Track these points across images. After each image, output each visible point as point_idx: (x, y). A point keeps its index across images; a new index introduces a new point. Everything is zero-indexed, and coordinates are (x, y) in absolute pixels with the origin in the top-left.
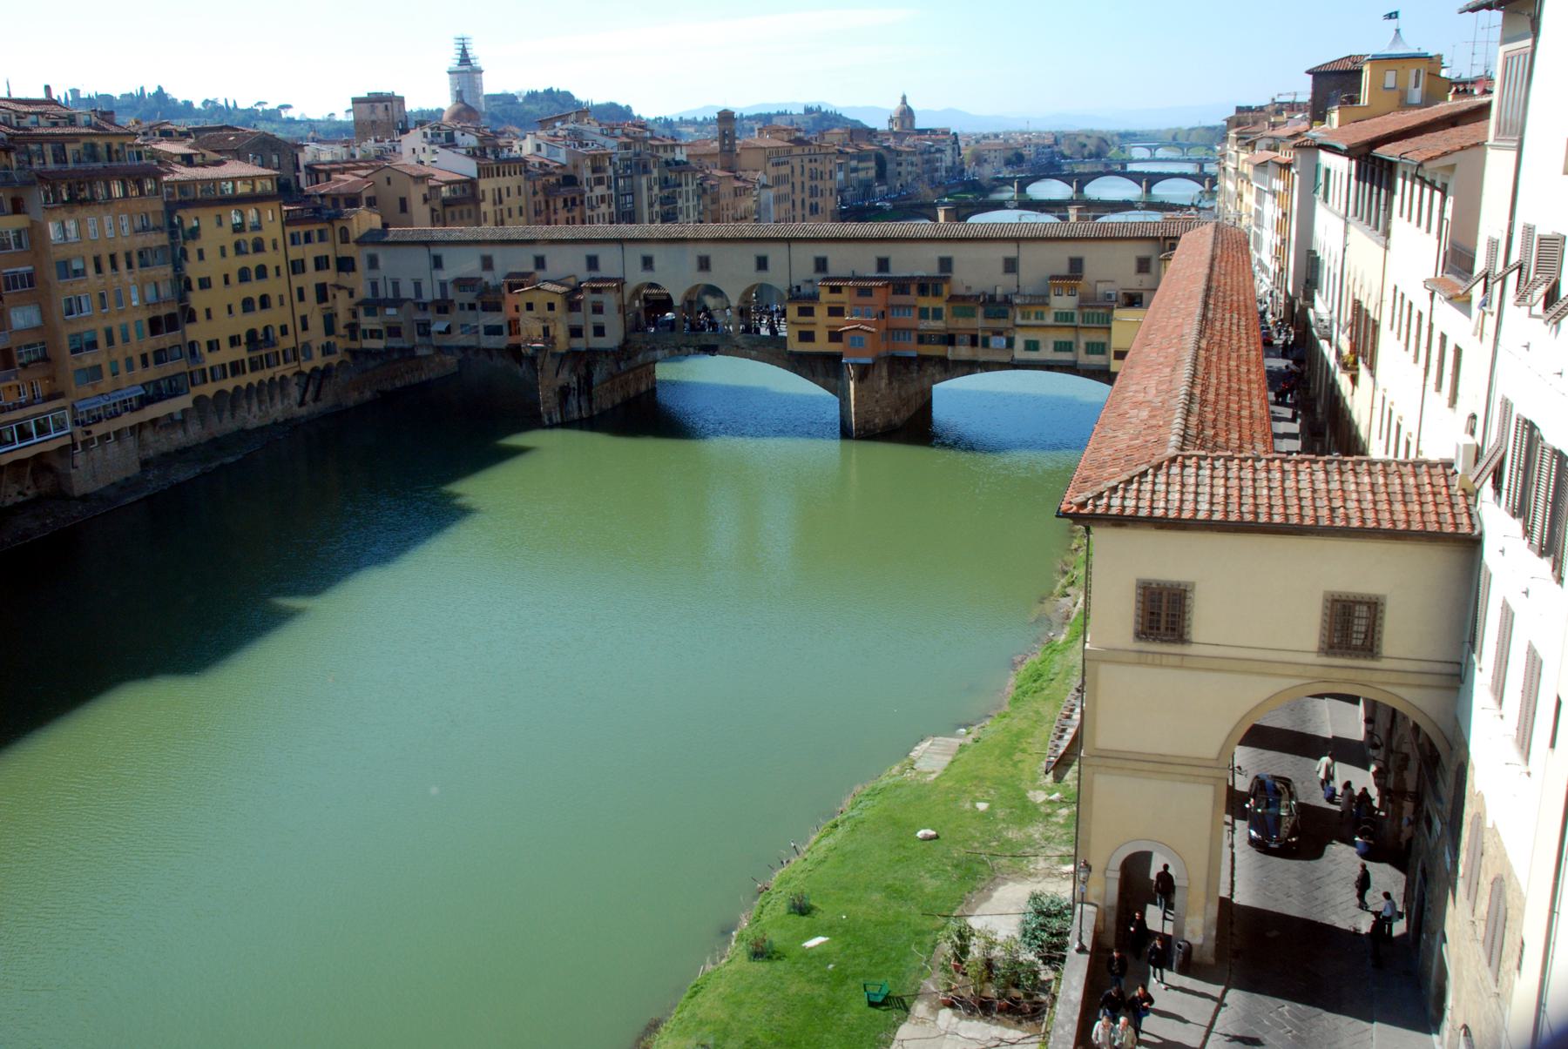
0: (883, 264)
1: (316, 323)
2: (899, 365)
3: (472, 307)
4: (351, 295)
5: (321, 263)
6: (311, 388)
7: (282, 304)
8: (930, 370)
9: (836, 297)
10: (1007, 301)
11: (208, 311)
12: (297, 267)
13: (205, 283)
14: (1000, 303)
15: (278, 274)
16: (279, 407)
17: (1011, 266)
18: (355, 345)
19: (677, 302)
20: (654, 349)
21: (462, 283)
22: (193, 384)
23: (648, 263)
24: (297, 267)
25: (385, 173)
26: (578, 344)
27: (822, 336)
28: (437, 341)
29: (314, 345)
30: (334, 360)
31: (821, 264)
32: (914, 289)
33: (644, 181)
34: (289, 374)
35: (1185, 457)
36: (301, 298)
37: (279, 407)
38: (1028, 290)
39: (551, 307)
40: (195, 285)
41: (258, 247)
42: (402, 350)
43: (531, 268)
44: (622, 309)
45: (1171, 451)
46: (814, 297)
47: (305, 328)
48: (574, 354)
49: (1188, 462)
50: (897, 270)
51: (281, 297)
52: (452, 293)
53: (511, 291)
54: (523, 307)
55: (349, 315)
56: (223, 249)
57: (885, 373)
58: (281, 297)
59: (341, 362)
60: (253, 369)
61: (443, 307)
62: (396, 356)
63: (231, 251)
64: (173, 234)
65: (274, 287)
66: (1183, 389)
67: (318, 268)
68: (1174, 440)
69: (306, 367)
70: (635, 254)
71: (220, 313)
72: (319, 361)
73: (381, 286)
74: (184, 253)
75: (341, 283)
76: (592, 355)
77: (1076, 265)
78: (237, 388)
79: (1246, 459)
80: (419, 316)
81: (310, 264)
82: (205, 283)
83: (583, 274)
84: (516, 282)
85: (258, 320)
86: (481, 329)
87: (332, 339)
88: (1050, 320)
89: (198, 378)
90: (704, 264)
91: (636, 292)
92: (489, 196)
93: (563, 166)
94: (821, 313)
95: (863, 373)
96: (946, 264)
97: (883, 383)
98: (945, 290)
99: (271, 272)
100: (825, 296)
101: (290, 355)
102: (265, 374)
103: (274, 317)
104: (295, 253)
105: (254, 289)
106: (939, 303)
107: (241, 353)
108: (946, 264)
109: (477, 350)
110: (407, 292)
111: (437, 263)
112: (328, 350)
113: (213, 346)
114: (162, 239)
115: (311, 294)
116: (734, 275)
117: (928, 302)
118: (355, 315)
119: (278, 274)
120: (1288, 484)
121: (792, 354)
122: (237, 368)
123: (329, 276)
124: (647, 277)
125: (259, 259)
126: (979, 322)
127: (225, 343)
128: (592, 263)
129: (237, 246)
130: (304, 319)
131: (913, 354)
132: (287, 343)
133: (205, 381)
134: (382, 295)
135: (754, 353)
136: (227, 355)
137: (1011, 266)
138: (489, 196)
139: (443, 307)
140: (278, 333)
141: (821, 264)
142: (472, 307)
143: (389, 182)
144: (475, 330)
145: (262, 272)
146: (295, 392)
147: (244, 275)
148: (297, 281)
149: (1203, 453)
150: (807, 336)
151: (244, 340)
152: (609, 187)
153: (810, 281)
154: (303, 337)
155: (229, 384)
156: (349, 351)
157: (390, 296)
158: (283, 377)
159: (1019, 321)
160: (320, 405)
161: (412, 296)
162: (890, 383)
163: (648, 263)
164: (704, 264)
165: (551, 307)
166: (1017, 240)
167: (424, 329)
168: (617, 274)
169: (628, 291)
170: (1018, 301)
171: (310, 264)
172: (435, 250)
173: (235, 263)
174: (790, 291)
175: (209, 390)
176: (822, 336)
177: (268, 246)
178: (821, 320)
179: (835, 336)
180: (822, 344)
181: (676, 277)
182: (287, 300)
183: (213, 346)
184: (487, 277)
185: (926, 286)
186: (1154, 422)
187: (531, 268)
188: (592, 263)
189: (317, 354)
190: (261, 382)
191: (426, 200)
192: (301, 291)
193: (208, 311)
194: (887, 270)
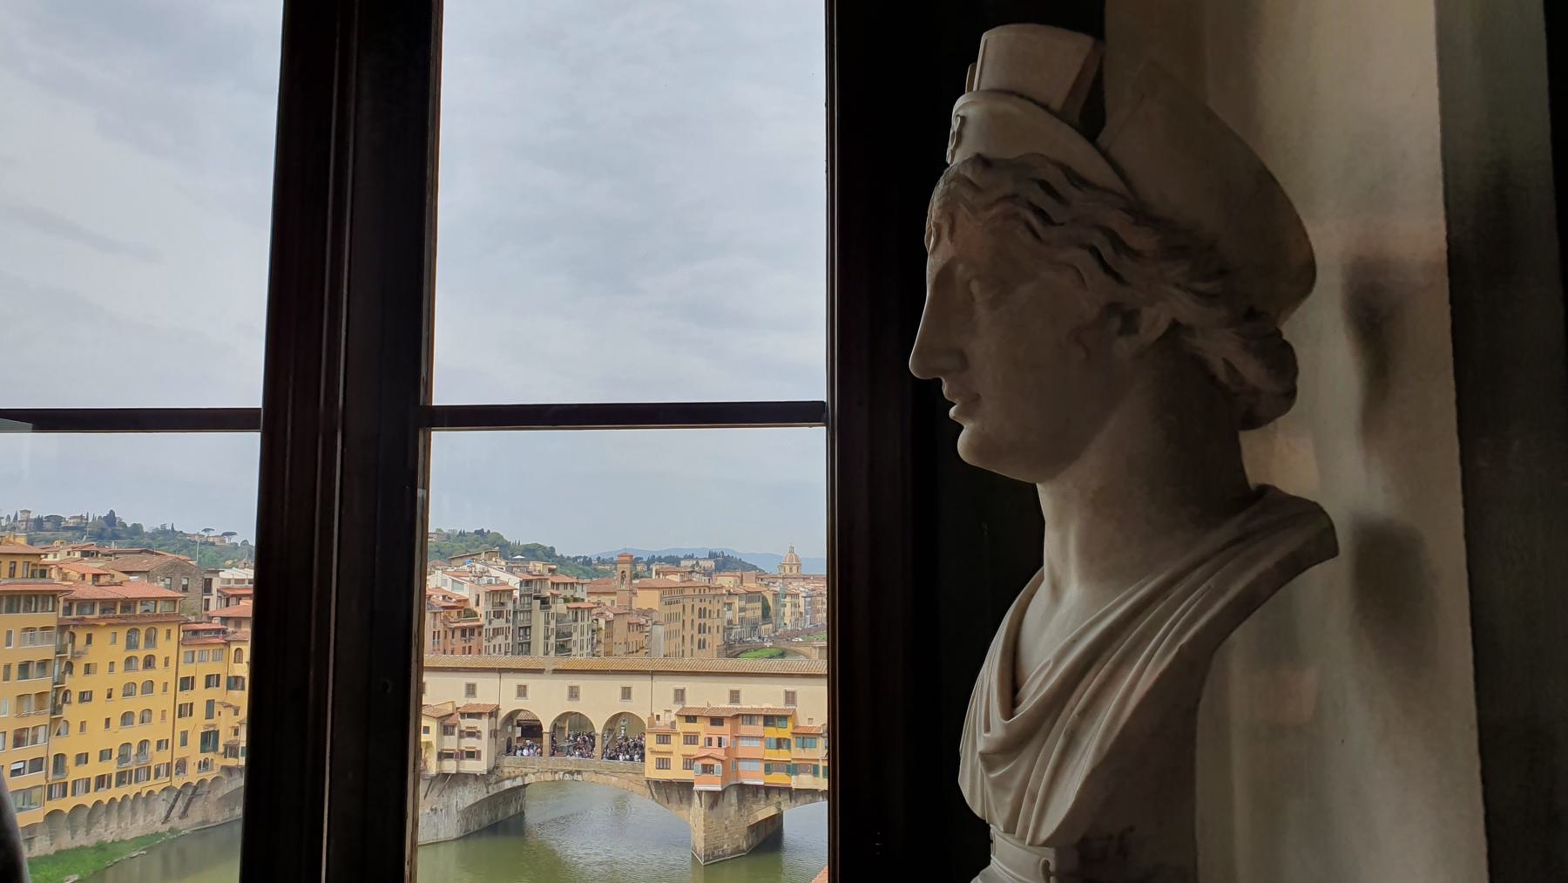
0: (735, 696)
1: (195, 741)
2: (747, 792)
5: (211, 681)
6: (180, 805)
7: (163, 717)
8: (775, 798)
9: (691, 727)
11: (83, 723)
12: (187, 683)
13: (85, 697)
15: (165, 690)
16: (141, 822)
19: (546, 728)
22: (50, 798)
23: (522, 691)
24: (187, 683)
26: (450, 766)
27: (677, 763)
30: (209, 776)
31: (680, 695)
32: (761, 723)
34: (157, 790)
37: (141, 822)
40: (75, 697)
44: (494, 734)
46: (673, 724)
47: (184, 742)
48: (443, 776)
50: (746, 704)
56: (8, 667)
57: (734, 800)
60: (120, 782)
63: (120, 667)
64: (60, 651)
67: (208, 686)
69: (178, 782)
70: (511, 682)
71: (96, 726)
72: (193, 776)
74: (70, 666)
75: (228, 701)
76: (460, 779)
78: (98, 803)
81: (200, 682)
82: (85, 697)
83: (462, 702)
85: (134, 734)
87: (210, 755)
89: (57, 791)
90: (574, 693)
91: (511, 716)
94: (677, 742)
95: (715, 798)
96: (790, 697)
97: (733, 810)
98: (790, 725)
99: (158, 687)
100: (684, 727)
101: (163, 770)
102: (130, 790)
105: (136, 704)
107: (111, 768)
108: (790, 697)
112: (204, 765)
113: (82, 759)
114: (46, 650)
116: (599, 702)
117: (773, 733)
119: (165, 690)
122: (102, 781)
125: (148, 675)
127: (94, 757)
128: (471, 690)
129: (129, 660)
130: (184, 735)
132: (163, 757)
133: (65, 795)
136: (94, 769)
141: (680, 695)
145: (149, 687)
146: (161, 809)
147: (129, 691)
148: (184, 697)
150: (663, 764)
151: (115, 755)
154: (180, 753)
155: (88, 800)
158: (150, 793)
160: (188, 822)
162: (740, 809)
163: (522, 691)
164: (574, 693)
169: (500, 719)
171: (200, 682)
173: (121, 678)
175: (66, 804)
176: (677, 763)
177: (159, 662)
178: (677, 747)
179: (689, 763)
180: (676, 773)
181: (546, 701)
183: (82, 759)
185: (769, 719)
188: (471, 690)
190: (125, 797)
193: (83, 723)
194: (737, 701)
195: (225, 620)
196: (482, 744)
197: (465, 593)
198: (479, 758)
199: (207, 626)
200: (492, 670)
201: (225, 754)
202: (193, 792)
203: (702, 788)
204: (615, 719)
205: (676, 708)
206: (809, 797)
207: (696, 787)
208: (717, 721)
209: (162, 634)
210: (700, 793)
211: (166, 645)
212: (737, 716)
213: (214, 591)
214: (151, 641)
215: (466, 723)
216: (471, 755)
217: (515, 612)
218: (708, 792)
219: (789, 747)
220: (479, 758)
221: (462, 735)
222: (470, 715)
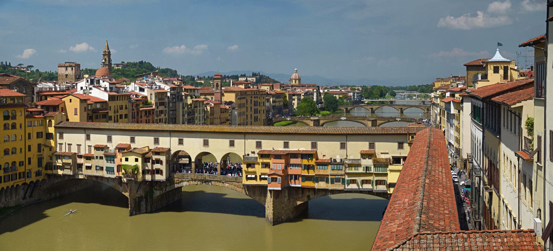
0: (286, 145)
1: (34, 161)
3: (101, 158)
4: (51, 150)
7: (21, 152)
8: (307, 193)
10: (342, 163)
14: (338, 164)
17: (343, 146)
18: (49, 172)
19: (193, 160)
20: (182, 181)
21: (97, 148)
23: (181, 142)
25: (70, 97)
26: (148, 177)
28: (85, 172)
29: (33, 171)
30: (40, 178)
31: (259, 145)
33: (181, 104)
35: (421, 234)
36: (30, 150)
38: (352, 158)
39: (137, 160)
41: (14, 126)
42: (69, 176)
43: (128, 142)
44: (167, 162)
45: (415, 233)
48: (144, 181)
49: (422, 237)
51: (21, 149)
52: (93, 152)
53: (119, 151)
54: (124, 159)
55: (49, 158)
57: (287, 194)
58: (21, 149)
59: (43, 180)
61: (88, 158)
62: (67, 178)
65: (19, 145)
66: (419, 203)
67: (37, 137)
68: (417, 227)
72: (34, 178)
73: (63, 146)
75: (47, 144)
76: (154, 183)
77: (372, 146)
79: (448, 233)
80: (80, 161)
83: (153, 147)
84: (121, 149)
85: (10, 159)
86: (105, 168)
87: (40, 169)
88: (361, 170)
90: (206, 143)
92: (112, 109)
93: (146, 97)
95: (276, 194)
96: (314, 146)
101: (22, 175)
103: (18, 158)
104: (29, 130)
106: (312, 162)
108: (314, 146)
109: (102, 178)
110: (74, 150)
111: (88, 138)
112: (38, 174)
115: (34, 149)
116: (219, 148)
118: (51, 158)
120: (466, 244)
121: (244, 185)
123: (41, 141)
124: (180, 148)
126: (328, 171)
128: (156, 141)
129: (5, 125)
130: (30, 159)
131: (300, 186)
132: (21, 169)
134: (63, 150)
135: (227, 184)
137: (343, 146)
138: (112, 109)
139: (88, 158)
140: (17, 165)
141: (259, 145)
142: (101, 158)
143: (71, 100)
144: (102, 168)
149: (429, 232)
152: (165, 107)
153: (253, 153)
154: (28, 167)
156: (47, 174)
157: (67, 151)
159: (347, 171)
161: (77, 152)
162: (289, 199)
163: (181, 142)
164: (206, 143)
165: (137, 160)
166: (347, 135)
167: (80, 166)
168: (167, 146)
170: (347, 162)
172: (87, 132)
174: (244, 156)
177: (18, 126)
178: (259, 169)
181: (193, 147)
182: (23, 150)
184: (109, 145)
186: (407, 219)
187: (129, 143)
189: (33, 175)
191: (85, 110)
192: (29, 147)
195: (42, 107)
196: (163, 167)
197: (145, 93)
198: (162, 174)
199: (36, 110)
200: (166, 131)
201: (46, 168)
202: (34, 185)
203: (271, 189)
204: (227, 155)
205: (257, 151)
206: (324, 193)
207: (268, 188)
208: (278, 156)
209: (18, 114)
210: (270, 191)
211: (20, 119)
212: (288, 154)
213: (35, 93)
214: (14, 117)
215: (155, 157)
216: (159, 172)
217: (169, 103)
218: (274, 190)
219: (314, 169)
220: (162, 174)
221: (153, 163)
222: (157, 153)
